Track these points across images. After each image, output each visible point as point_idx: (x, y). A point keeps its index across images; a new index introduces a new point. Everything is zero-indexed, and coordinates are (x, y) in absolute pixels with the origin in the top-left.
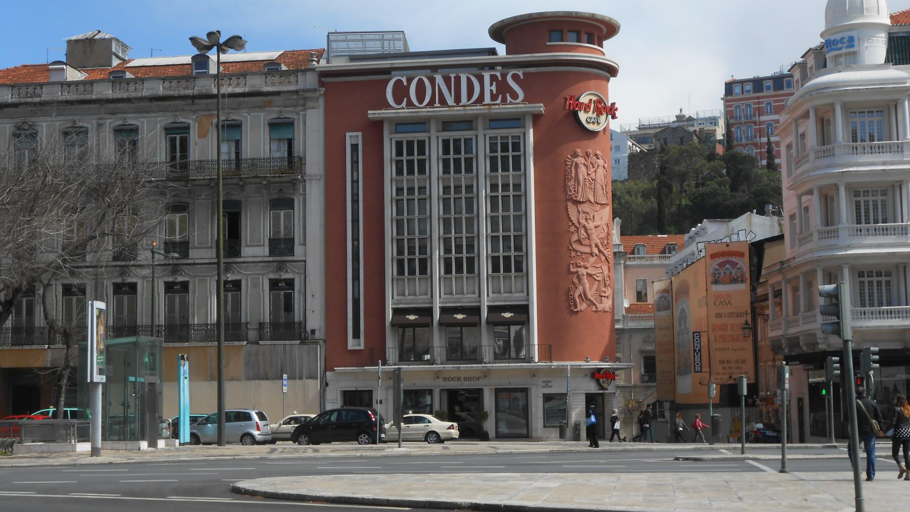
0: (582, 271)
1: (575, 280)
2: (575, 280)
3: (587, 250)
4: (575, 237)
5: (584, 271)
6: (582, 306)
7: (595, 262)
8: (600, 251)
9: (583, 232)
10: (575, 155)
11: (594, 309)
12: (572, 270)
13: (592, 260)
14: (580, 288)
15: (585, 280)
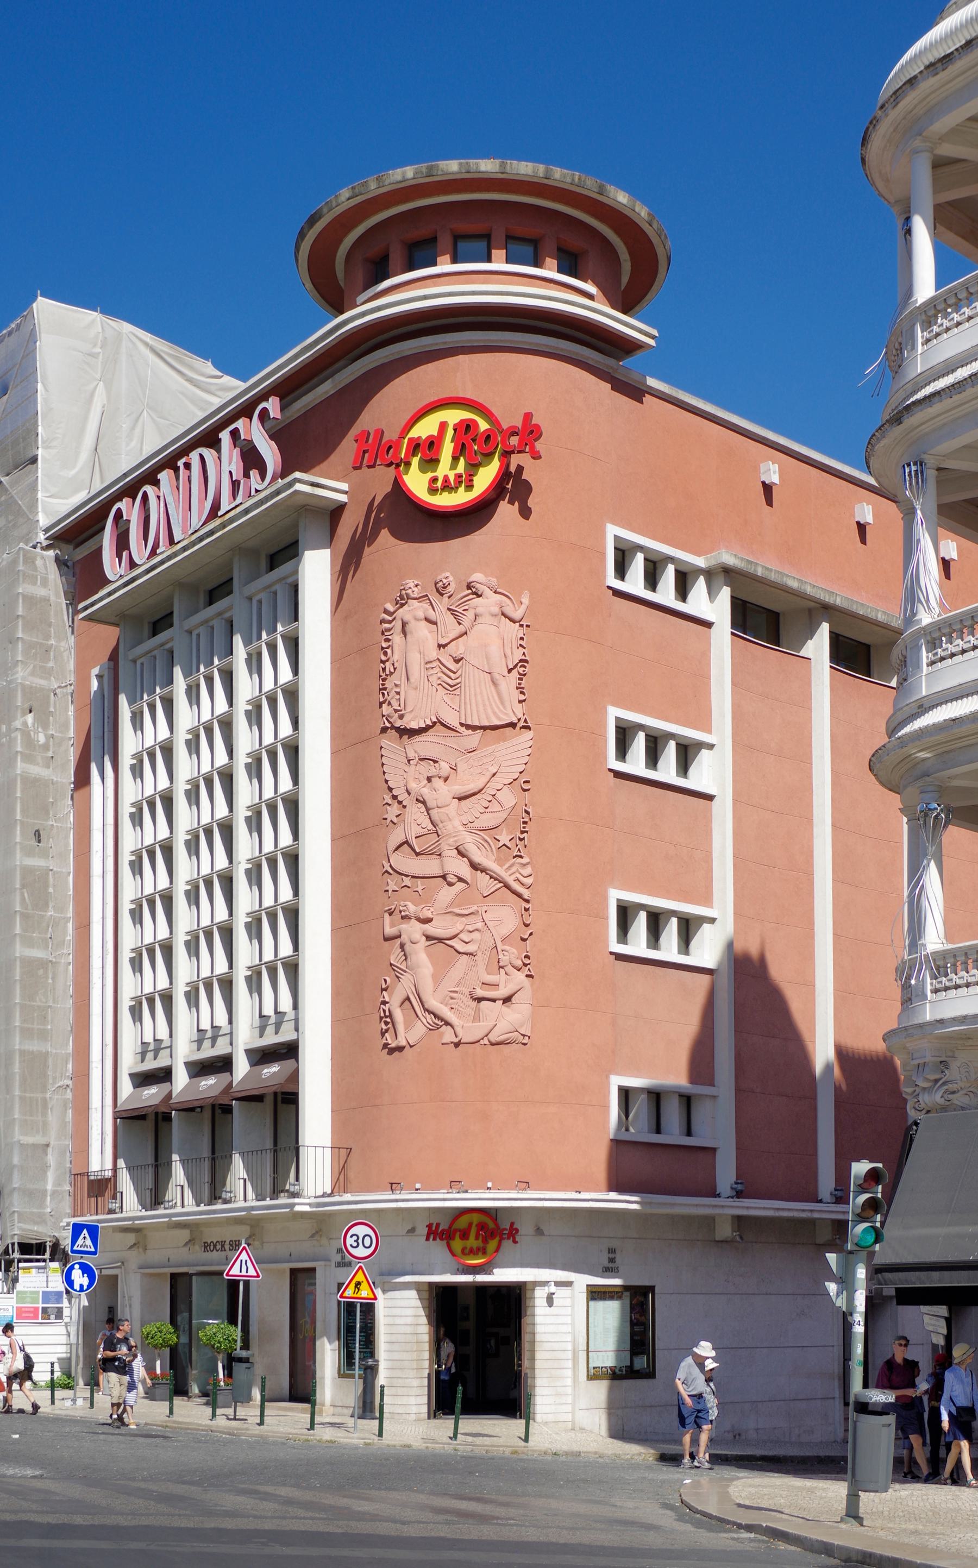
0: (413, 930)
1: (395, 957)
2: (395, 957)
3: (430, 866)
4: (396, 837)
5: (413, 930)
6: (410, 1031)
7: (458, 900)
8: (474, 866)
9: (415, 813)
10: (402, 601)
11: (448, 1035)
12: (389, 931)
13: (446, 894)
14: (406, 980)
15: (421, 955)
